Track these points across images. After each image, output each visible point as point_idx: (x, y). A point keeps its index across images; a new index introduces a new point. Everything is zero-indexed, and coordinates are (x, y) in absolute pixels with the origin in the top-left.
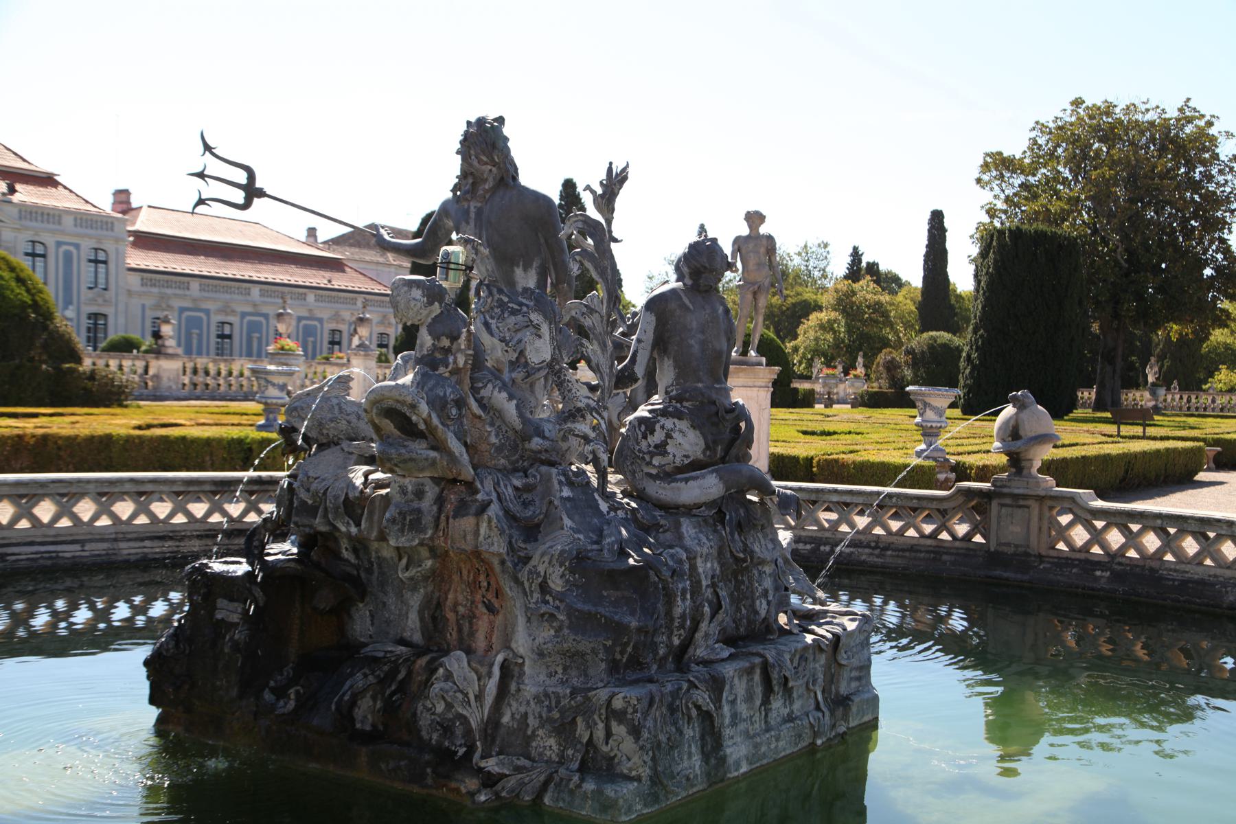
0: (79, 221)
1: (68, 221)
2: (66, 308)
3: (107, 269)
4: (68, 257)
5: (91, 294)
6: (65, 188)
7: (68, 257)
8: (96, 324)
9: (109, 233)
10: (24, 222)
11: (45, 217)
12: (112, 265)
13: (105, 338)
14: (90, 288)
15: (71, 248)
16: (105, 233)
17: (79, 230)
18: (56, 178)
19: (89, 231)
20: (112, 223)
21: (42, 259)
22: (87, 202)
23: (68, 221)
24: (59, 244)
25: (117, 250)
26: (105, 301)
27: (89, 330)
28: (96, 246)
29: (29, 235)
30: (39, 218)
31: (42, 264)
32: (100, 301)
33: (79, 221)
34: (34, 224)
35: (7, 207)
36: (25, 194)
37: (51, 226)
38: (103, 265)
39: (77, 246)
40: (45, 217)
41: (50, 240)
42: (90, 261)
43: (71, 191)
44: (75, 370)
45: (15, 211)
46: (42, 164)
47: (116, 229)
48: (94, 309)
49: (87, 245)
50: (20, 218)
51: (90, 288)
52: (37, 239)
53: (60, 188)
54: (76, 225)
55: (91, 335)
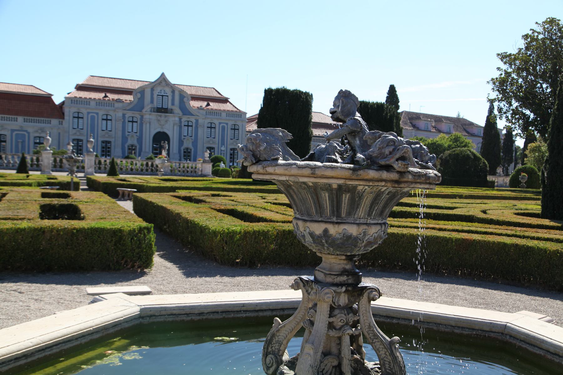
0: (228, 115)
1: (224, 115)
2: (221, 146)
3: (112, 123)
4: (223, 128)
5: (232, 141)
6: (230, 103)
7: (223, 128)
8: (234, 152)
9: (240, 118)
10: (207, 116)
11: (215, 114)
12: (240, 130)
13: (214, 154)
14: (231, 139)
16: (238, 118)
17: (228, 118)
18: (229, 100)
19: (232, 118)
20: (241, 115)
21: (136, 123)
22: (236, 107)
23: (224, 115)
24: (220, 123)
25: (242, 124)
26: (80, 134)
27: (231, 154)
28: (234, 124)
29: (209, 121)
30: (213, 114)
31: (111, 123)
32: (235, 144)
33: (228, 115)
34: (211, 116)
35: (201, 111)
36: (213, 105)
37: (217, 117)
38: (110, 121)
39: (227, 124)
40: (215, 114)
41: (217, 122)
43: (231, 104)
44: (219, 170)
45: (204, 112)
47: (242, 117)
48: (233, 147)
49: (230, 123)
50: (206, 114)
51: (231, 139)
52: (212, 122)
53: (228, 104)
54: (227, 116)
55: (232, 156)
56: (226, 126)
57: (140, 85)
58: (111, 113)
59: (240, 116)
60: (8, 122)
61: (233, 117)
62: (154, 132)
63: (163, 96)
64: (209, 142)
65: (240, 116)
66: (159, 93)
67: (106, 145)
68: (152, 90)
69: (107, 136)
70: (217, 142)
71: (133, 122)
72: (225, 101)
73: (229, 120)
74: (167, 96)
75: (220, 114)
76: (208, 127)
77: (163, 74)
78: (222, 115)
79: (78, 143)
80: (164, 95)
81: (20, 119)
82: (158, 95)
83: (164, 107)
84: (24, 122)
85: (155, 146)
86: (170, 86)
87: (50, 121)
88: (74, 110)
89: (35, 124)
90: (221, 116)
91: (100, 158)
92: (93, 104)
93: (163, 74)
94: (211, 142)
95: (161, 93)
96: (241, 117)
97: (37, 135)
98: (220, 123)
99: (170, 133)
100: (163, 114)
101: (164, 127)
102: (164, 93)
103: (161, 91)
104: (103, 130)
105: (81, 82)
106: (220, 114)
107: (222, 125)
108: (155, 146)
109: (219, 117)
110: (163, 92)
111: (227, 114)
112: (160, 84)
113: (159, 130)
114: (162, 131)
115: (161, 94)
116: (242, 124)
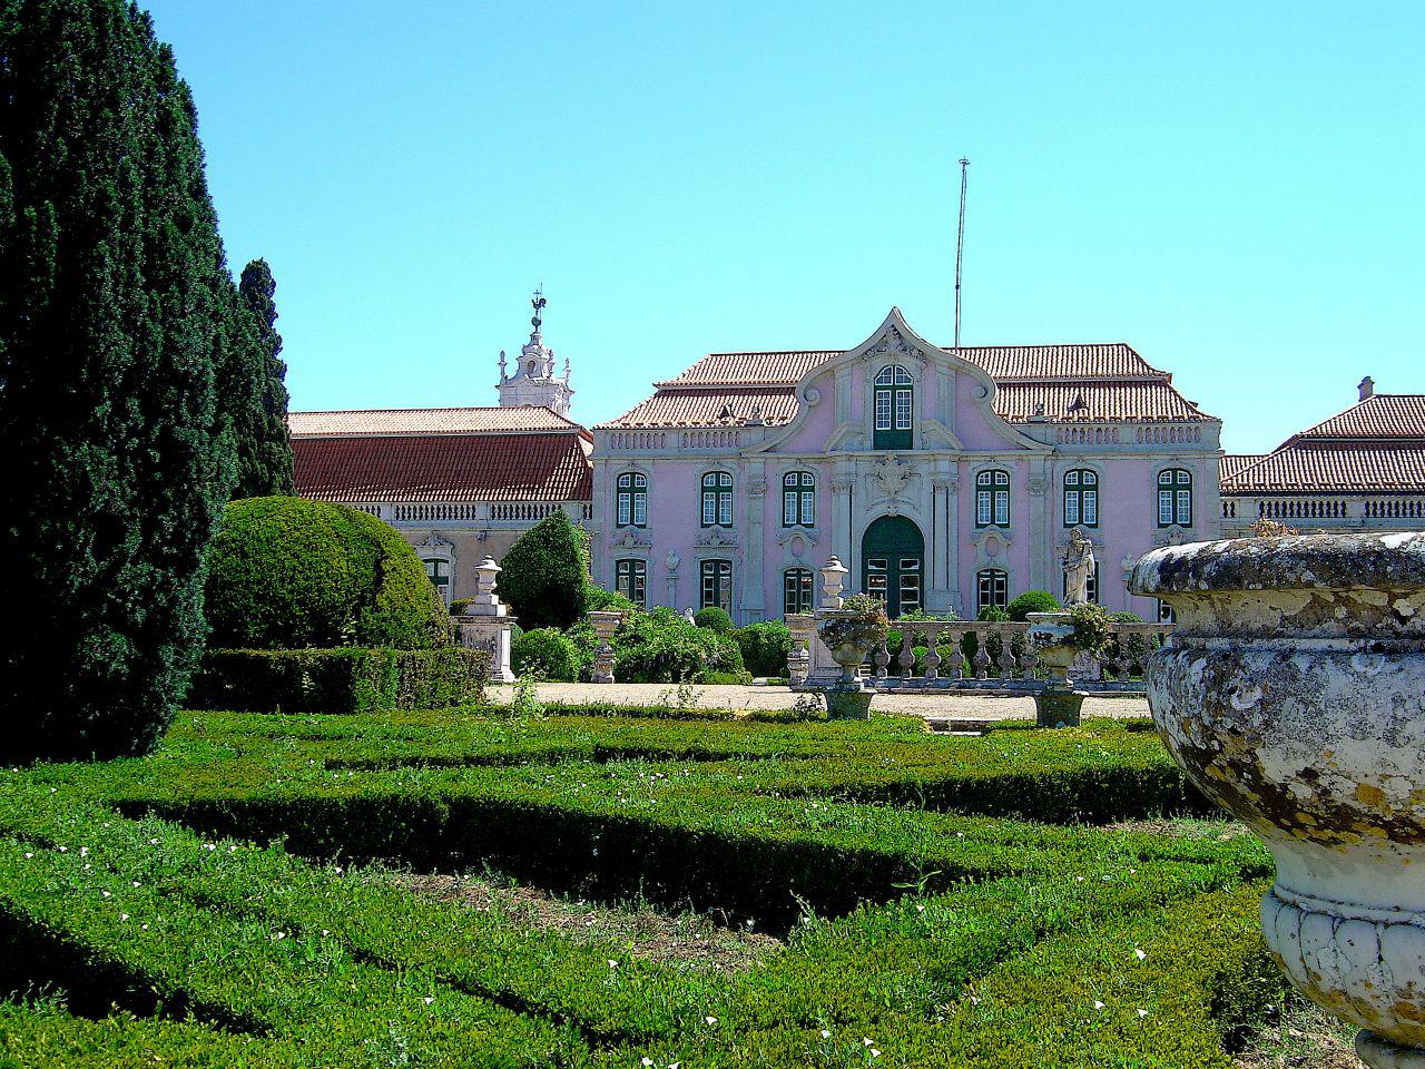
1: (1127, 434)
36: (1101, 403)
46: (1158, 363)
57: (809, 364)
58: (729, 465)
62: (863, 522)
63: (894, 388)
67: (716, 575)
69: (715, 542)
71: (718, 489)
72: (1162, 381)
74: (911, 388)
77: (894, 313)
79: (632, 574)
85: (870, 567)
86: (915, 352)
88: (620, 466)
91: (698, 612)
92: (672, 439)
93: (894, 313)
97: (625, 554)
99: (922, 521)
100: (891, 454)
105: (672, 375)
108: (870, 567)
113: (880, 511)
114: (892, 513)
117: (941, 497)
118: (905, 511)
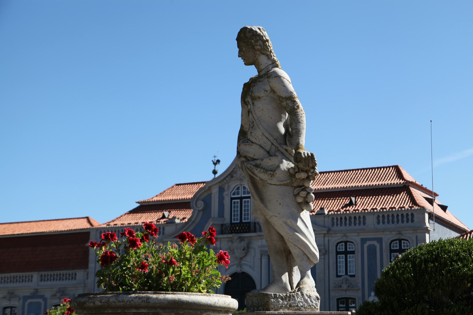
0: (381, 219)
1: (371, 221)
4: (372, 250)
7: (372, 250)
9: (410, 223)
15: (375, 243)
19: (391, 225)
24: (363, 241)
25: (417, 237)
33: (381, 219)
37: (357, 227)
39: (380, 240)
42: (353, 252)
47: (415, 219)
49: (387, 237)
52: (345, 239)
54: (378, 223)
56: (378, 246)
59: (410, 217)
60: (21, 284)
61: (393, 222)
63: (241, 198)
64: (341, 287)
65: (410, 217)
66: (234, 194)
68: (221, 190)
70: (360, 285)
73: (383, 231)
74: (249, 197)
75: (362, 219)
76: (353, 252)
78: (367, 221)
80: (243, 196)
81: (36, 276)
82: (232, 199)
83: (243, 221)
84: (41, 280)
87: (76, 274)
89: (52, 283)
90: (364, 224)
94: (345, 286)
95: (238, 194)
96: (412, 221)
98: (363, 241)
99: (254, 274)
100: (235, 236)
101: (243, 262)
102: (244, 193)
103: (238, 188)
104: (338, 276)
106: (362, 219)
107: (368, 243)
109: (362, 226)
110: (241, 190)
111: (378, 216)
112: (232, 177)
114: (238, 270)
115: (240, 196)
116: (417, 237)
117: (264, 260)
118: (246, 269)
